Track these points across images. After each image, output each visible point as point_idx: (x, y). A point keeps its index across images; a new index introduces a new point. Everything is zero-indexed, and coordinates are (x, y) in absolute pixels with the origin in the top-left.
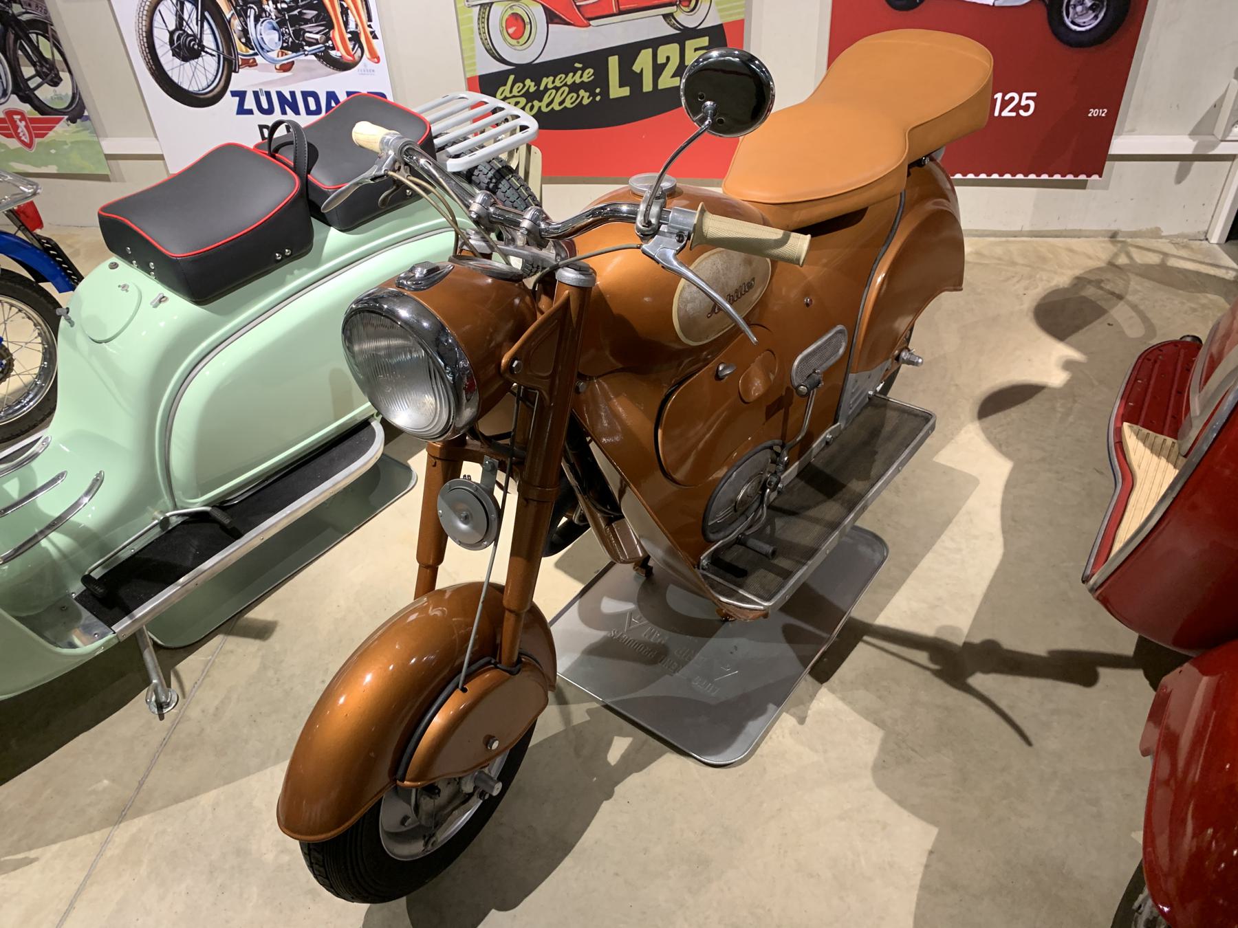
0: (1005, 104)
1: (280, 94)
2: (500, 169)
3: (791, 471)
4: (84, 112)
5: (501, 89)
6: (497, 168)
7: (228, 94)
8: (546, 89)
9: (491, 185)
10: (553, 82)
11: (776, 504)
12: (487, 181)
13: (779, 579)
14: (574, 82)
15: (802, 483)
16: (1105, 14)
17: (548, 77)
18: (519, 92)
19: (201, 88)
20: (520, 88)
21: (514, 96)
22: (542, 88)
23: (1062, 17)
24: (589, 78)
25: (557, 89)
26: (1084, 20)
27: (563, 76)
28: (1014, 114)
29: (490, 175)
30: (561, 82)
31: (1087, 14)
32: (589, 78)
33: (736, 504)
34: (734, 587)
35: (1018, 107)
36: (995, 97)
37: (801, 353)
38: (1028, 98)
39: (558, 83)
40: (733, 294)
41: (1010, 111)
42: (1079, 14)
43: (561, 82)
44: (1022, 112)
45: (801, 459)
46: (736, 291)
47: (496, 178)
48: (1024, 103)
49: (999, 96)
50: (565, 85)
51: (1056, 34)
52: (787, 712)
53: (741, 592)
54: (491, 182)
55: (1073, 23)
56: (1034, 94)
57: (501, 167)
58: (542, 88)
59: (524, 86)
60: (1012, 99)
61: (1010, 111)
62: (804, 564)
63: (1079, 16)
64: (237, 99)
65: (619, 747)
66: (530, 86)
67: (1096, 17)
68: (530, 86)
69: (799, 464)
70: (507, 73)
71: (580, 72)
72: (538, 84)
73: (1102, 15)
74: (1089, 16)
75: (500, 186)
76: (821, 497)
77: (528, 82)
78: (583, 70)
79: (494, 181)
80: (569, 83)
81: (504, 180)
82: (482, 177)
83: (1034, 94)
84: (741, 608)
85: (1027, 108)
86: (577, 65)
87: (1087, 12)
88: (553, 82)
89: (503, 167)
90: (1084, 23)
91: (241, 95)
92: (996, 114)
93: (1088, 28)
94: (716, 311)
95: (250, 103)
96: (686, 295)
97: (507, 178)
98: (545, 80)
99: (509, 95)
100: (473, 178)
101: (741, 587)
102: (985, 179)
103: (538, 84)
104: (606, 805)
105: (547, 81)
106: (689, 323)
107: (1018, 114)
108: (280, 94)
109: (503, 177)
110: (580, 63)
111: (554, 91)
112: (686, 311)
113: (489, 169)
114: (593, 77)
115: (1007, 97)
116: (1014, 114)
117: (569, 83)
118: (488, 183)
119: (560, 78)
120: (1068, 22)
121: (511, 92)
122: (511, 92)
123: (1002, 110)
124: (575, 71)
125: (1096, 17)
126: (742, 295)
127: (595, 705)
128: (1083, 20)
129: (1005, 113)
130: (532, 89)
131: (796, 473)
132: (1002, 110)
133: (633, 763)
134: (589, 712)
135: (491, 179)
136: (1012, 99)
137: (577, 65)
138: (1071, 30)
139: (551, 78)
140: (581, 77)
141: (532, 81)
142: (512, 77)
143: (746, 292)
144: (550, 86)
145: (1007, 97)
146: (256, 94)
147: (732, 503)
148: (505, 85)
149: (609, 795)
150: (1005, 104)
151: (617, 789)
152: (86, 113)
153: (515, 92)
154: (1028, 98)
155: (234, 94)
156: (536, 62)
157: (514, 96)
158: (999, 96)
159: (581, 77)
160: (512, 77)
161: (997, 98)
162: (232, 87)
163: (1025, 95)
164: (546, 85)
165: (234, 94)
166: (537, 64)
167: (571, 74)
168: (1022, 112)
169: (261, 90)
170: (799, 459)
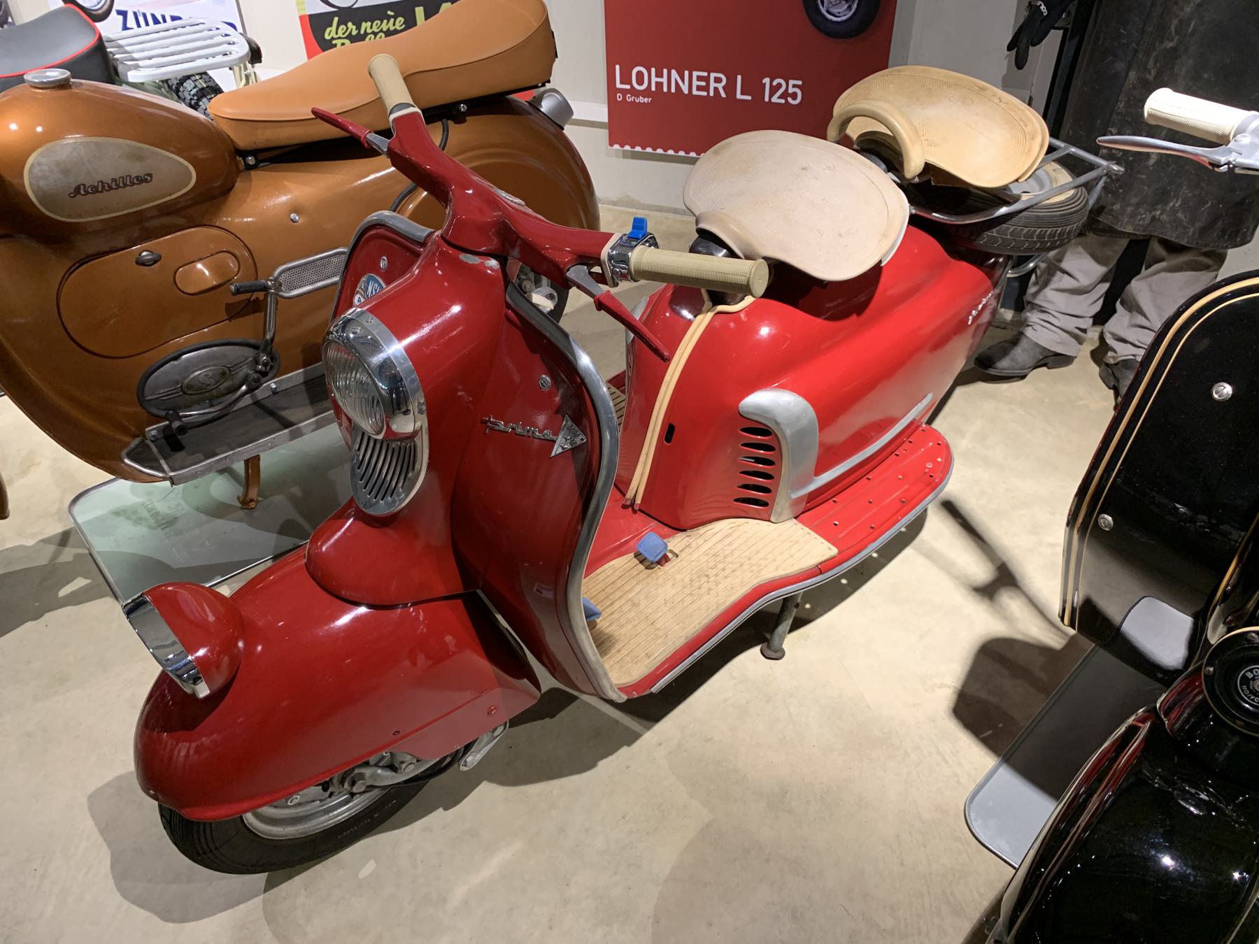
0: (774, 90)
1: (153, 16)
2: (203, 89)
3: (292, 376)
4: (7, 19)
5: (328, 30)
6: (200, 87)
7: (114, 13)
8: (366, 34)
9: (193, 102)
10: (371, 27)
11: (265, 402)
12: (189, 97)
13: (202, 458)
14: (389, 29)
15: (303, 388)
16: (858, 5)
17: (366, 22)
18: (343, 34)
19: (93, 5)
20: (344, 30)
21: (339, 38)
22: (362, 32)
23: (817, 5)
24: (401, 26)
25: (375, 34)
26: (839, 10)
27: (379, 22)
28: (783, 101)
29: (192, 93)
30: (378, 28)
31: (841, 5)
32: (401, 26)
33: (181, 386)
34: (159, 456)
35: (785, 95)
36: (764, 81)
37: (284, 264)
38: (794, 86)
39: (375, 29)
40: (110, 182)
41: (779, 98)
42: (833, 3)
43: (378, 28)
44: (790, 99)
45: (309, 368)
46: (114, 180)
47: (197, 96)
48: (791, 90)
49: (767, 81)
50: (381, 31)
51: (813, 22)
52: (228, 585)
53: (162, 462)
54: (193, 99)
55: (828, 12)
56: (800, 83)
57: (205, 86)
58: (362, 32)
59: (347, 28)
60: (779, 85)
61: (779, 98)
62: (233, 450)
63: (833, 5)
64: (121, 17)
65: (79, 583)
66: (352, 30)
67: (850, 8)
68: (352, 30)
69: (304, 371)
70: (332, 15)
71: (392, 20)
72: (359, 28)
73: (855, 6)
74: (843, 5)
75: (201, 103)
76: (307, 401)
77: (350, 24)
78: (395, 17)
79: (196, 98)
80: (385, 30)
81: (205, 99)
82: (186, 94)
83: (800, 83)
84: (141, 471)
85: (794, 96)
86: (390, 13)
87: (840, 3)
88: (371, 27)
89: (207, 87)
90: (839, 13)
91: (123, 14)
92: (767, 99)
93: (844, 18)
94: (82, 192)
95: (131, 22)
96: (36, 170)
97: (208, 97)
98: (364, 25)
99: (335, 36)
100: (180, 93)
101: (165, 458)
102: (672, 155)
103: (359, 28)
104: (30, 624)
105: (365, 26)
106: (46, 198)
107: (786, 100)
108: (153, 16)
109: (204, 96)
110: (392, 11)
111: (373, 36)
112: (39, 187)
113: (192, 87)
114: (404, 26)
115: (775, 83)
116: (783, 101)
117: (385, 30)
118: (191, 99)
119: (377, 25)
120: (824, 11)
121: (337, 33)
122: (337, 33)
123: (771, 96)
124: (389, 18)
125: (850, 8)
126: (125, 185)
127: (87, 552)
128: (840, 13)
129: (775, 99)
130: (354, 33)
131: (301, 380)
132: (771, 96)
133: (76, 599)
134: (77, 556)
135: (193, 96)
136: (779, 85)
137: (390, 13)
138: (827, 19)
139: (369, 23)
140: (394, 25)
141: (353, 24)
142: (336, 19)
143: (133, 184)
144: (369, 31)
145: (775, 83)
146: (135, 14)
147: (178, 384)
148: (331, 26)
149: (37, 617)
150: (774, 90)
151: (47, 615)
152: (10, 20)
153: (340, 34)
154: (794, 86)
155: (119, 12)
156: (355, 6)
157: (339, 38)
158: (767, 81)
159: (394, 25)
160: (336, 19)
161: (765, 84)
162: (115, 7)
163: (792, 82)
164: (365, 30)
165: (119, 12)
166: (355, 8)
167: (385, 21)
168: (790, 99)
169: (139, 11)
170: (305, 366)
